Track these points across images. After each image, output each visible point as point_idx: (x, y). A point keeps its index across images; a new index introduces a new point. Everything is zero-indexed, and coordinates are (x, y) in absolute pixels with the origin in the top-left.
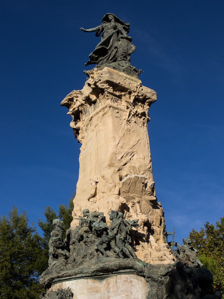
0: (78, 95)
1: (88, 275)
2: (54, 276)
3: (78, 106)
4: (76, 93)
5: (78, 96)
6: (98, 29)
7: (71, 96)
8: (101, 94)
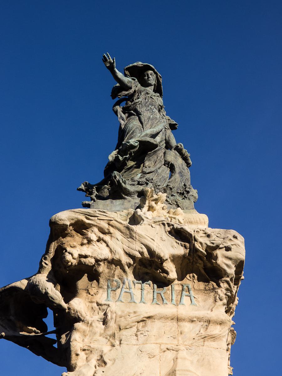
0: (112, 230)
4: (111, 223)
6: (129, 85)
8: (196, 277)
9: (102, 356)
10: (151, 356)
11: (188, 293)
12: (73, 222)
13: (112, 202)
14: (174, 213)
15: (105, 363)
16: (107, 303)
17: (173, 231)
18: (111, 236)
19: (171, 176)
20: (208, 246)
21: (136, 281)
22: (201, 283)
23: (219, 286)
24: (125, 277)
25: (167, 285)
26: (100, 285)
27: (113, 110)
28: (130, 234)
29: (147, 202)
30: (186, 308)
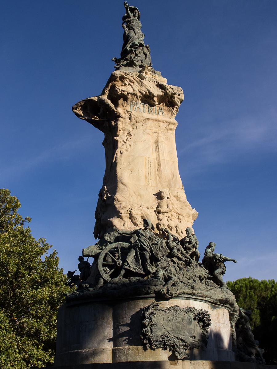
1: (211, 300)
2: (187, 291)
3: (129, 92)
4: (134, 78)
5: (134, 82)
7: (125, 75)
8: (165, 104)
9: (129, 132)
10: (148, 134)
11: (161, 111)
12: (120, 76)
13: (128, 68)
14: (155, 76)
15: (131, 135)
16: (131, 111)
17: (158, 85)
18: (134, 84)
19: (146, 59)
20: (172, 93)
21: (141, 103)
22: (166, 107)
23: (173, 109)
24: (138, 101)
25: (154, 107)
26: (128, 103)
27: (122, 26)
28: (141, 84)
29: (145, 70)
30: (161, 117)
